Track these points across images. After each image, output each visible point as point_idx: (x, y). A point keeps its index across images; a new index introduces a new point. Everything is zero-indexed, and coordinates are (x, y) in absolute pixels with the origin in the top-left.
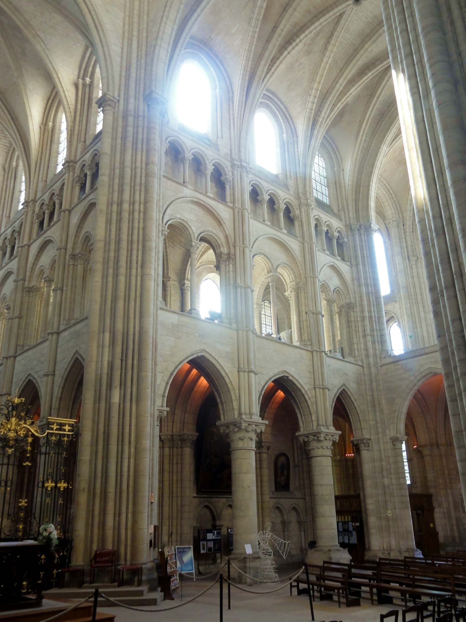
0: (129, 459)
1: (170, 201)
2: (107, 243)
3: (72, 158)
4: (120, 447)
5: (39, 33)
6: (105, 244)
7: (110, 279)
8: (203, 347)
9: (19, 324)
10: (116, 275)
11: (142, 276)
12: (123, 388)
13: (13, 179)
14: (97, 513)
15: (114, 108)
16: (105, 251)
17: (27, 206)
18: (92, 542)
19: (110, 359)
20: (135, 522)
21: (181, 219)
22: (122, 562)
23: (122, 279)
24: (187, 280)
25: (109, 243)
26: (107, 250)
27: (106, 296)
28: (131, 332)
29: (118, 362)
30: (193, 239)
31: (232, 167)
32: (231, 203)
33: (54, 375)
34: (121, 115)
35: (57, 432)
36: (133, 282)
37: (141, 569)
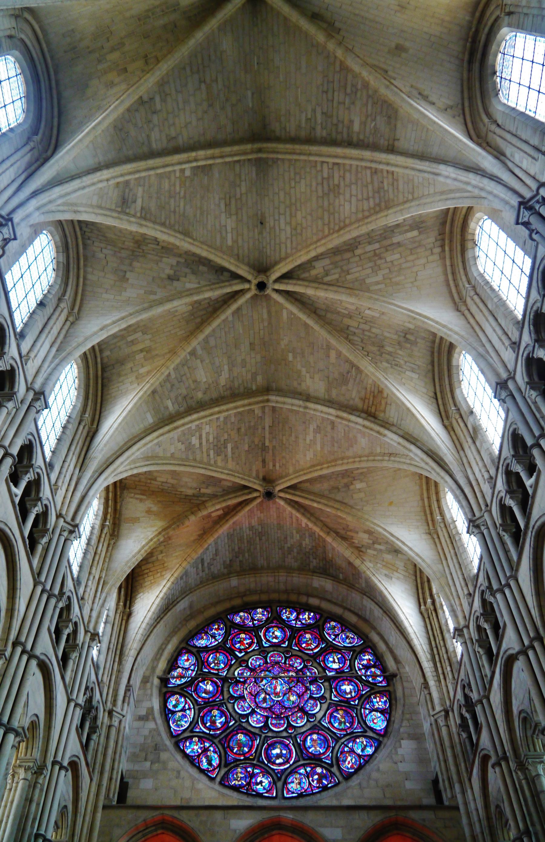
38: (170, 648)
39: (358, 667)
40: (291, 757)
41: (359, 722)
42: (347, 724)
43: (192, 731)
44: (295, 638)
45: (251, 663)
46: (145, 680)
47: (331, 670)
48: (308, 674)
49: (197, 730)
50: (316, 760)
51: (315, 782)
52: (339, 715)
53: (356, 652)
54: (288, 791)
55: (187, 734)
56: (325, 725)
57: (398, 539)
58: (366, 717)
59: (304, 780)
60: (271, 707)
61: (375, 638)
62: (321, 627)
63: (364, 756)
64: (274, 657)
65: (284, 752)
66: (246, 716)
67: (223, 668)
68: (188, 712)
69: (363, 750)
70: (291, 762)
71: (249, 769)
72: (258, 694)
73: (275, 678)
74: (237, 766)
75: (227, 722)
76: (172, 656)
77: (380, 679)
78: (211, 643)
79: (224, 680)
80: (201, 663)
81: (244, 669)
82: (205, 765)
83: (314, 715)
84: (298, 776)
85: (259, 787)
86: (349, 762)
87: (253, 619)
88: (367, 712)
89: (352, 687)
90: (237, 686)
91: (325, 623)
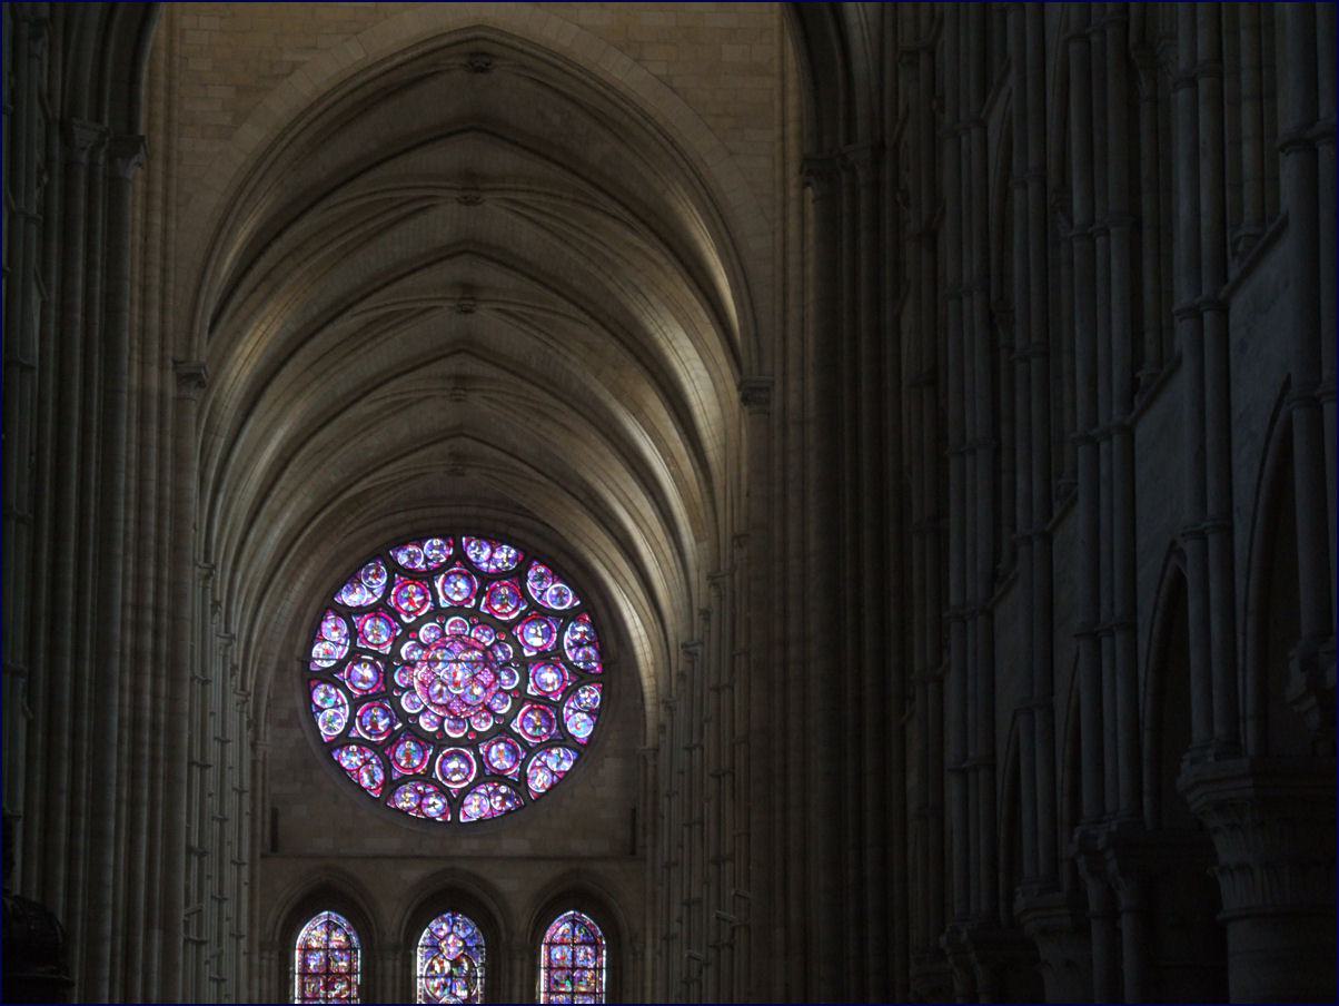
15: (768, 402)
38: (311, 612)
39: (568, 644)
40: (471, 772)
41: (558, 727)
42: (544, 730)
43: (347, 737)
44: (485, 593)
45: (424, 636)
46: (282, 667)
47: (531, 648)
48: (500, 654)
49: (353, 735)
50: (500, 777)
51: (498, 804)
54: (465, 815)
55: (341, 742)
56: (516, 730)
57: (620, 573)
58: (567, 719)
59: (484, 802)
60: (449, 703)
61: (597, 601)
62: (523, 575)
63: (560, 772)
64: (453, 625)
65: (463, 766)
66: (417, 716)
67: (385, 644)
68: (342, 709)
69: (558, 764)
70: (471, 780)
71: (420, 788)
72: (432, 684)
73: (457, 661)
74: (406, 783)
75: (391, 725)
76: (314, 620)
77: (594, 664)
78: (368, 601)
79: (387, 660)
80: (354, 634)
81: (413, 645)
82: (366, 781)
83: (501, 715)
84: (477, 797)
85: (431, 810)
86: (539, 782)
87: (427, 560)
88: (571, 712)
89: (555, 676)
90: (404, 671)
91: (529, 567)
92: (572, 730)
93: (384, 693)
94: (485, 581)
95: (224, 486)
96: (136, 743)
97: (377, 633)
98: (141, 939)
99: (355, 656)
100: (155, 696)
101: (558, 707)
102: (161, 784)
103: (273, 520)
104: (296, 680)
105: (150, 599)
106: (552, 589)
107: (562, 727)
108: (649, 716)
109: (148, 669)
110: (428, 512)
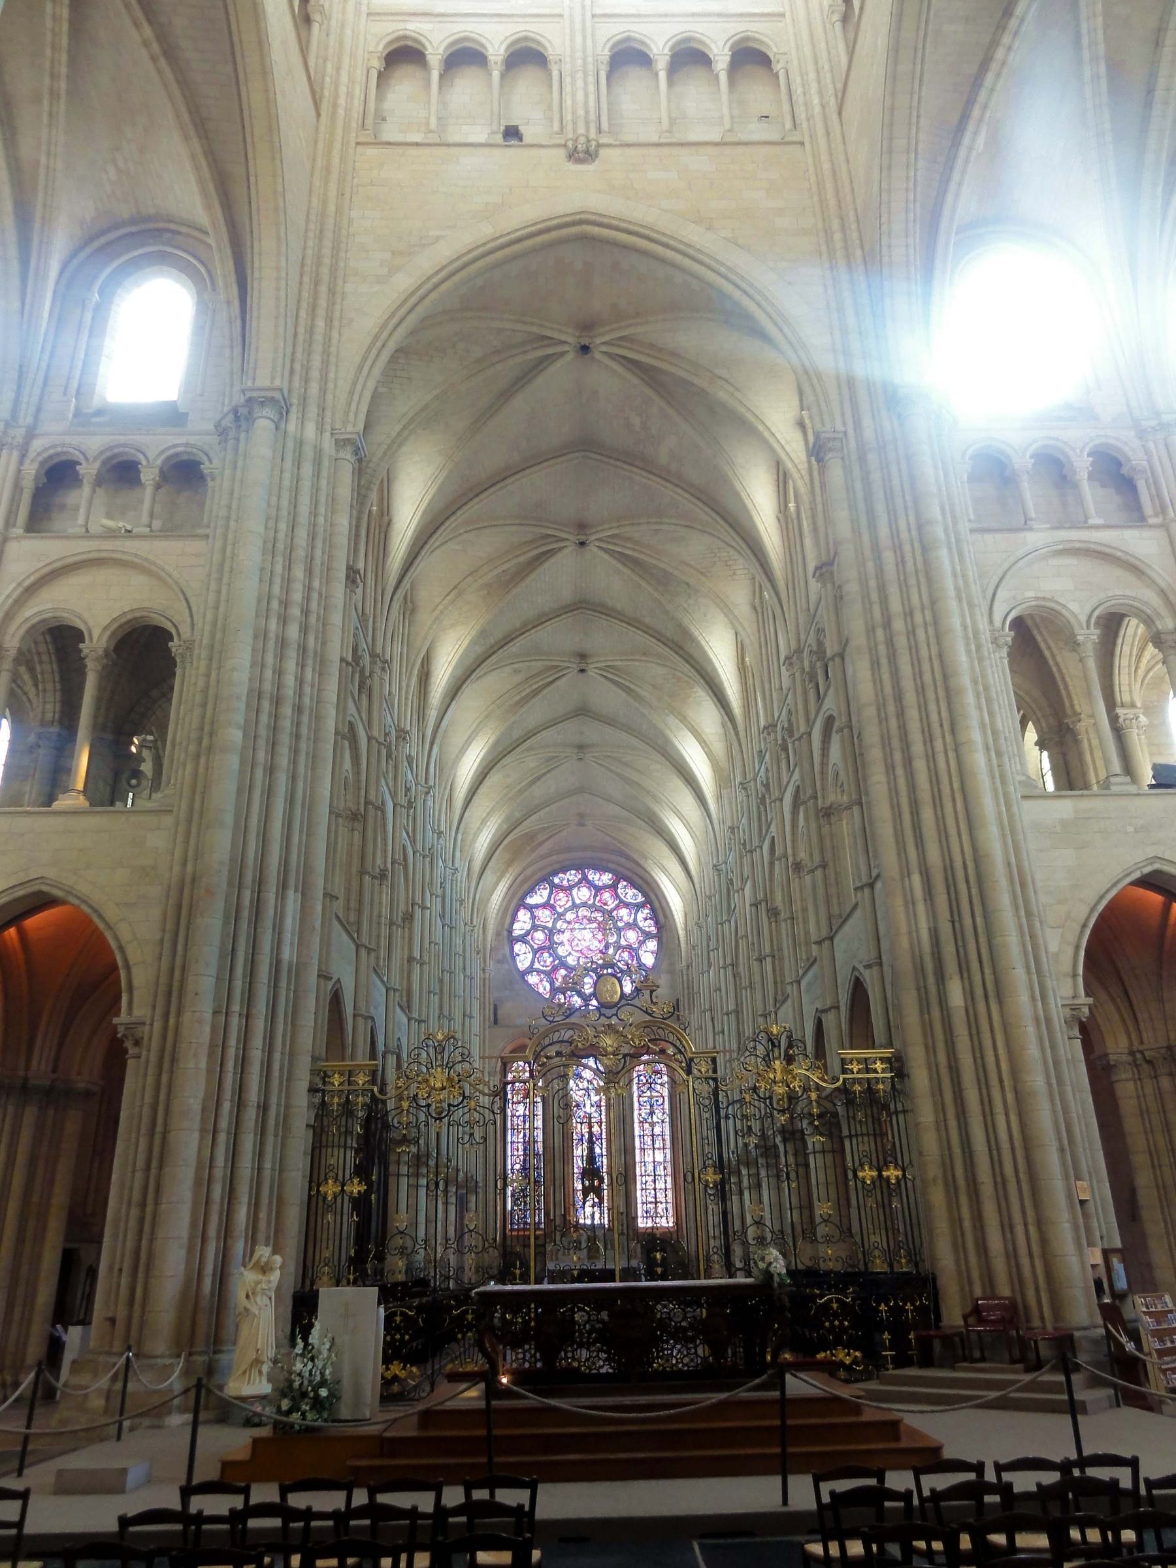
0: (1007, 1115)
1: (1000, 573)
2: (881, 706)
3: (824, 559)
4: (984, 1091)
5: (717, 372)
6: (878, 709)
7: (900, 771)
8: (1151, 852)
9: (825, 878)
10: (908, 761)
11: (956, 750)
12: (965, 975)
13: (771, 622)
14: (967, 1224)
16: (880, 722)
17: (791, 664)
18: (970, 1283)
19: (932, 925)
20: (1044, 1242)
21: (1037, 598)
22: (1036, 1323)
23: (920, 765)
24: (1122, 706)
25: (884, 705)
26: (883, 720)
27: (899, 806)
28: (958, 864)
29: (945, 929)
30: (1077, 630)
31: (1141, 438)
32: (1156, 515)
33: (881, 964)
34: (854, 457)
35: (860, 1076)
36: (942, 764)
37: (1071, 1337)
38: (513, 906)
46: (498, 934)
52: (625, 955)
53: (639, 907)
61: (653, 897)
64: (583, 912)
79: (551, 931)
80: (533, 917)
82: (541, 990)
92: (643, 961)
93: (550, 946)
94: (598, 890)
95: (437, 741)
96: (276, 716)
97: (544, 916)
98: (271, 897)
99: (535, 928)
100: (300, 681)
101: (636, 950)
102: (302, 759)
103: (484, 822)
104: (506, 942)
105: (297, 596)
106: (631, 892)
107: (638, 959)
108: (683, 950)
109: (292, 654)
110: (567, 856)
